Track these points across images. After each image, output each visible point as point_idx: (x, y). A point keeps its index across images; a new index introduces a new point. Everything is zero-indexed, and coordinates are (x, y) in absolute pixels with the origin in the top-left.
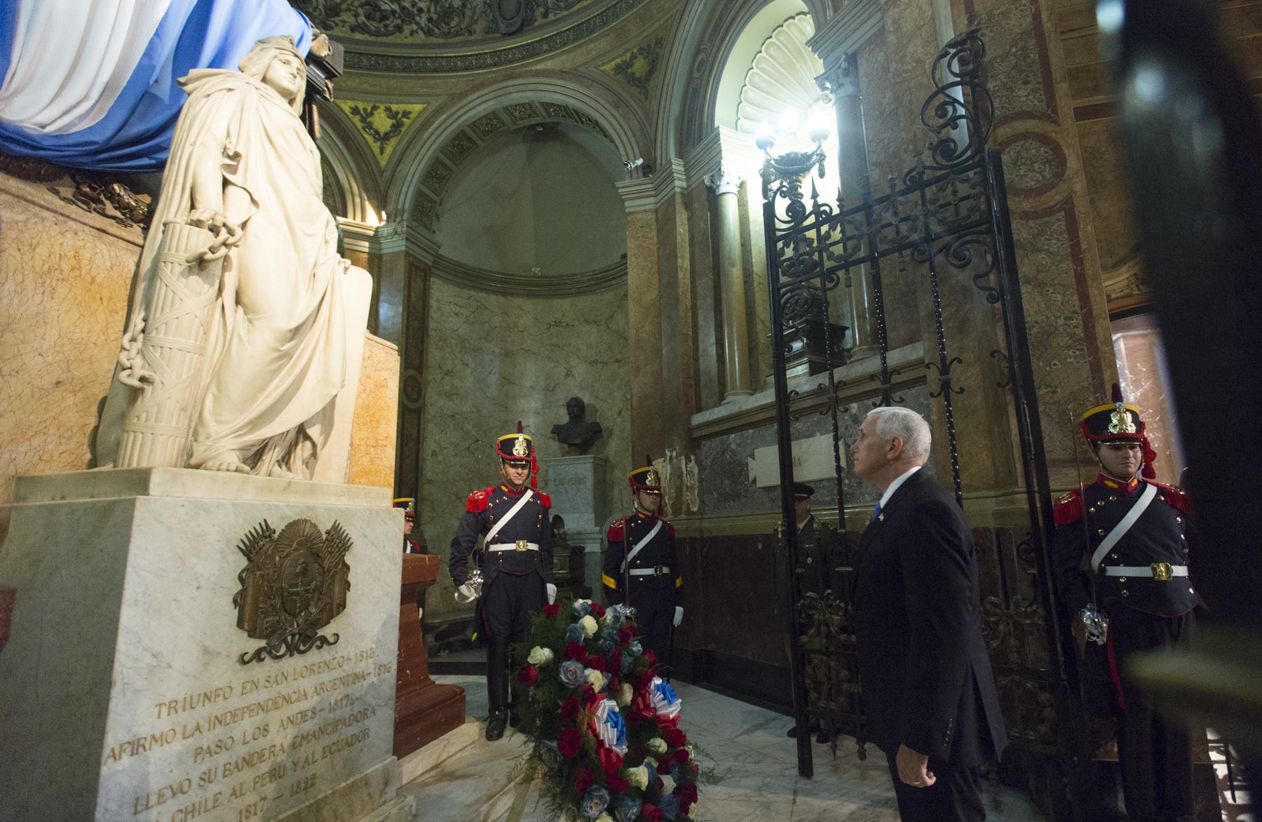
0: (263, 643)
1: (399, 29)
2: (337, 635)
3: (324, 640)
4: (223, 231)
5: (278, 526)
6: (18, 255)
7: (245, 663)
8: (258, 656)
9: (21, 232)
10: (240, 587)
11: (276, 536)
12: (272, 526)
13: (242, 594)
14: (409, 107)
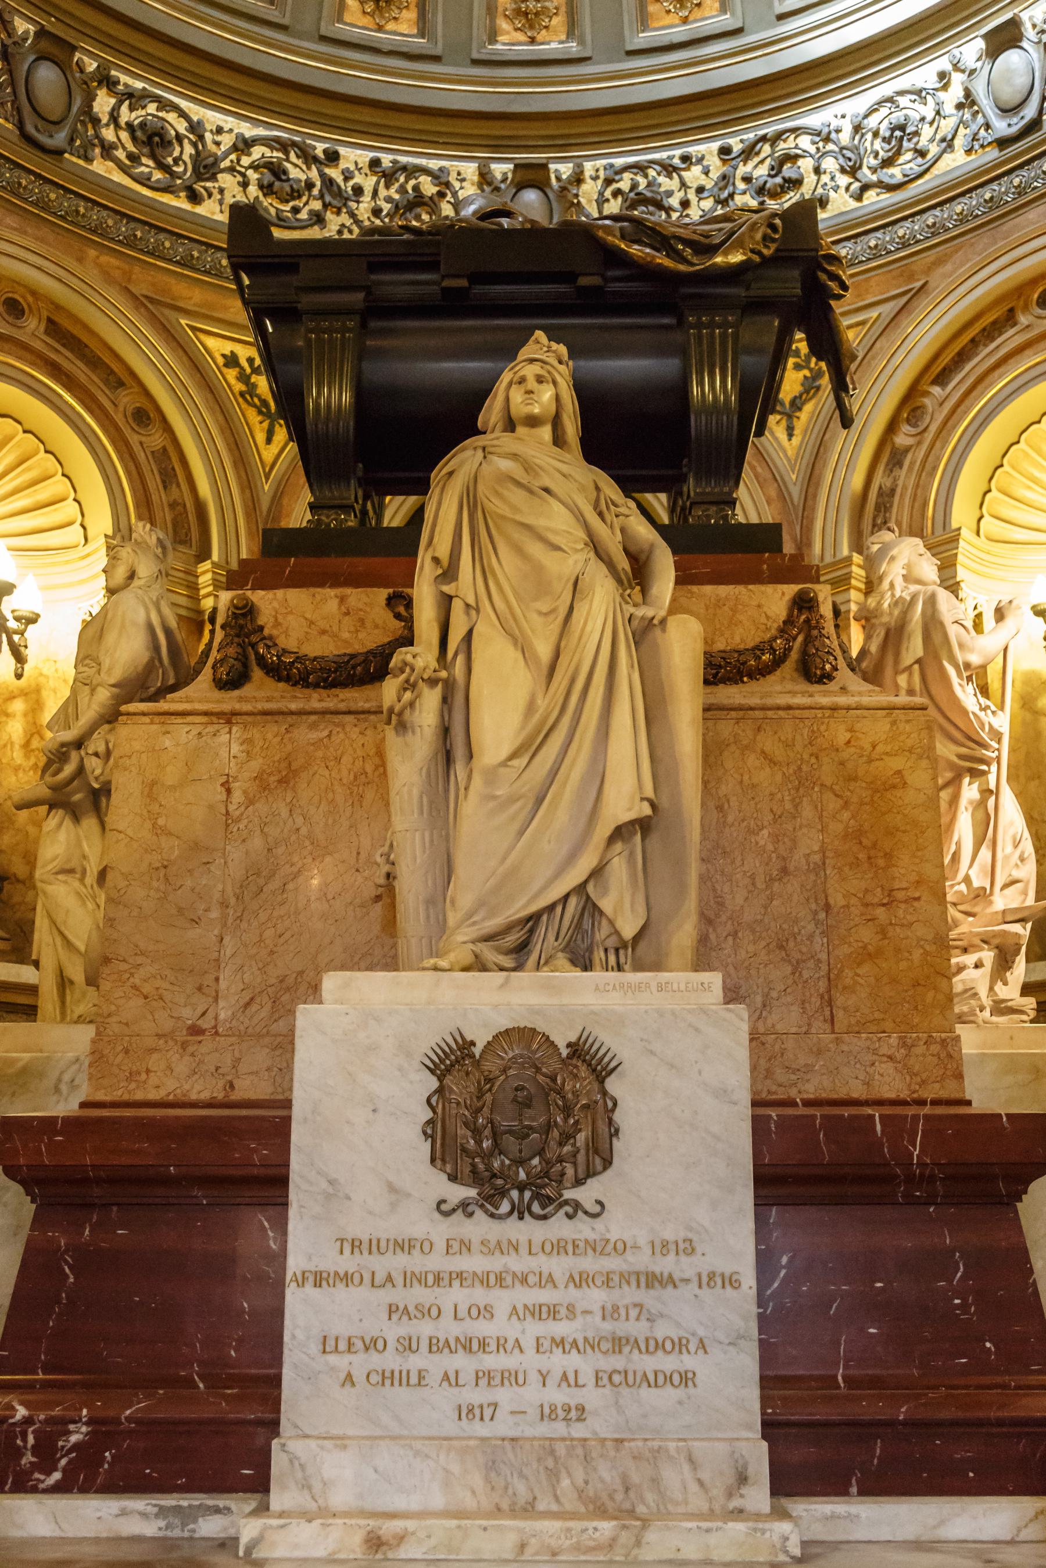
0: (472, 1193)
2: (600, 1203)
3: (577, 1206)
4: (408, 670)
5: (481, 1039)
6: (327, 773)
7: (447, 1214)
9: (327, 747)
10: (431, 1115)
11: (477, 1051)
12: (469, 1038)
13: (430, 1122)
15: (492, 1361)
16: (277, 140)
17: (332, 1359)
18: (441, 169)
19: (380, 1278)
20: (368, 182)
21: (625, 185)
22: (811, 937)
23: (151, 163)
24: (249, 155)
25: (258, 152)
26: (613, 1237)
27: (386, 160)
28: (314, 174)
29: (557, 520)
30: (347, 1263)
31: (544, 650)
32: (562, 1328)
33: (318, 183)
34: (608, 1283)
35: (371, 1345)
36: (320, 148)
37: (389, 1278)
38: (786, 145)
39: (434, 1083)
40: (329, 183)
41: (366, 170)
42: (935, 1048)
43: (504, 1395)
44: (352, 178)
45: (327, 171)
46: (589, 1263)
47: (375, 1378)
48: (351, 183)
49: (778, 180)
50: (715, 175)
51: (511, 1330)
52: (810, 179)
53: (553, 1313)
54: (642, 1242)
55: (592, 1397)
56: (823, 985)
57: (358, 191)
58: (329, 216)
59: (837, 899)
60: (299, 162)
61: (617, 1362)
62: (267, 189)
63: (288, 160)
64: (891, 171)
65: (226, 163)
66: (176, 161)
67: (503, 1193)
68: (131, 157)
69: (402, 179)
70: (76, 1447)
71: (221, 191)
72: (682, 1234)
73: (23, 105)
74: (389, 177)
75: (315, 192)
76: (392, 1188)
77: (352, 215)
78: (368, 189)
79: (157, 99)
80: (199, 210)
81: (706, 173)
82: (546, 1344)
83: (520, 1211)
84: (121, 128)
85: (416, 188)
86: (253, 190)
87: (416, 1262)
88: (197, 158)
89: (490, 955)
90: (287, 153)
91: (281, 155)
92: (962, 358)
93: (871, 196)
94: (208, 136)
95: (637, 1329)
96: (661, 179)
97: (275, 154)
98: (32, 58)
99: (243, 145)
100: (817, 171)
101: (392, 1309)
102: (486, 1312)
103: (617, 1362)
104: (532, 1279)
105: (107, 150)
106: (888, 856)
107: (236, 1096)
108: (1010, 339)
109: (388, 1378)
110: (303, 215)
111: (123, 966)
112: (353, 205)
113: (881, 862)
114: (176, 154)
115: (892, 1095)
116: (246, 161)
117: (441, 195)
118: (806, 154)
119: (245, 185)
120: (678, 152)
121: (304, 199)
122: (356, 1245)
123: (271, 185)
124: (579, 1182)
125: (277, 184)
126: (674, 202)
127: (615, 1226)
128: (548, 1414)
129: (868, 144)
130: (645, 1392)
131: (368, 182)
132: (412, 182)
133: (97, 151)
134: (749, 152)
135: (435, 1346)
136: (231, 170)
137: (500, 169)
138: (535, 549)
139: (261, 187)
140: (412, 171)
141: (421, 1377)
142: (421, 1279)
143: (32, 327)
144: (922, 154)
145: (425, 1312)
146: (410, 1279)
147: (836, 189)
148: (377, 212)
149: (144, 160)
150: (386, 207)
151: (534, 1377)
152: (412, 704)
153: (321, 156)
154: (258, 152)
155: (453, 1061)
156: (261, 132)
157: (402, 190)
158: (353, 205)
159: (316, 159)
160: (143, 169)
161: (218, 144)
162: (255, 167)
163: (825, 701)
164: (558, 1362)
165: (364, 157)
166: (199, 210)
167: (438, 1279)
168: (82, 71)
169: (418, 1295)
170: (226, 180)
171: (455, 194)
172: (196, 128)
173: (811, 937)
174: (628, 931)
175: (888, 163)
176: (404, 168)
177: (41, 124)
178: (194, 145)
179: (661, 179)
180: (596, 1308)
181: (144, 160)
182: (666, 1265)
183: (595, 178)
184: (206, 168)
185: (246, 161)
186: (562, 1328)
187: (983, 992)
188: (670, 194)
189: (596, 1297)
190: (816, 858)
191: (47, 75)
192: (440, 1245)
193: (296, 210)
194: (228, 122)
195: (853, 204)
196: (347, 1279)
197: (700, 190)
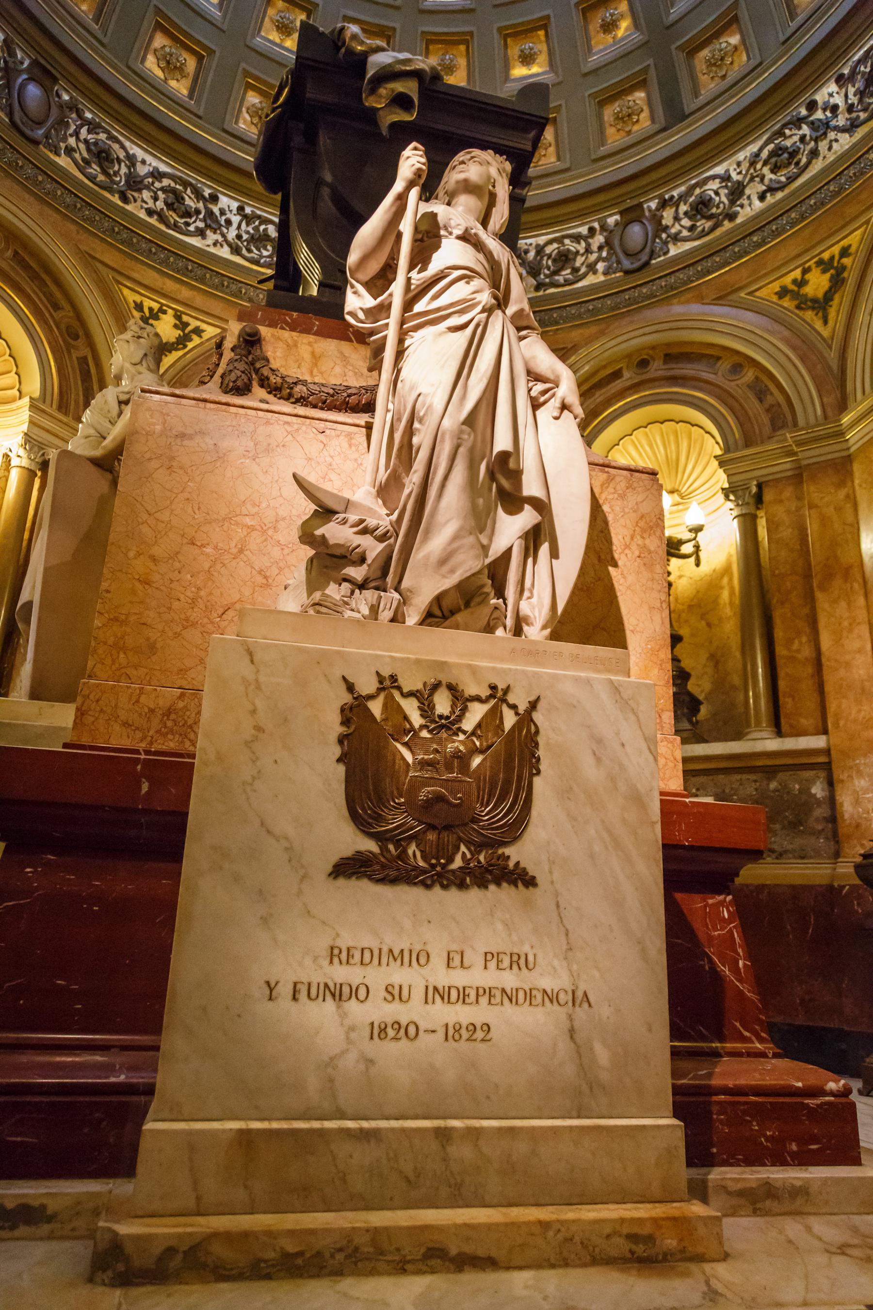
16: (180, 178)
20: (236, 219)
23: (98, 169)
24: (161, 182)
25: (166, 182)
27: (248, 210)
28: (201, 205)
33: (203, 211)
36: (207, 192)
40: (210, 214)
44: (225, 214)
45: (210, 206)
48: (224, 218)
57: (229, 222)
58: (208, 232)
60: (193, 196)
62: (169, 206)
63: (185, 193)
64: (557, 278)
68: (83, 159)
69: (257, 223)
73: (14, 104)
74: (248, 219)
75: (201, 216)
78: (235, 225)
79: (106, 131)
84: (80, 141)
85: (265, 230)
86: (160, 204)
90: (186, 190)
91: (181, 188)
97: (178, 187)
98: (25, 76)
99: (157, 175)
105: (69, 151)
110: (192, 228)
112: (225, 231)
119: (156, 199)
121: (193, 219)
123: (173, 204)
129: (544, 262)
131: (236, 219)
132: (262, 227)
139: (166, 203)
148: (239, 237)
150: (245, 237)
153: (207, 196)
154: (166, 182)
157: (256, 229)
158: (225, 231)
159: (203, 197)
160: (92, 171)
175: (556, 273)
176: (259, 217)
177: (25, 119)
185: (157, 185)
191: (33, 91)
193: (187, 224)
194: (149, 159)
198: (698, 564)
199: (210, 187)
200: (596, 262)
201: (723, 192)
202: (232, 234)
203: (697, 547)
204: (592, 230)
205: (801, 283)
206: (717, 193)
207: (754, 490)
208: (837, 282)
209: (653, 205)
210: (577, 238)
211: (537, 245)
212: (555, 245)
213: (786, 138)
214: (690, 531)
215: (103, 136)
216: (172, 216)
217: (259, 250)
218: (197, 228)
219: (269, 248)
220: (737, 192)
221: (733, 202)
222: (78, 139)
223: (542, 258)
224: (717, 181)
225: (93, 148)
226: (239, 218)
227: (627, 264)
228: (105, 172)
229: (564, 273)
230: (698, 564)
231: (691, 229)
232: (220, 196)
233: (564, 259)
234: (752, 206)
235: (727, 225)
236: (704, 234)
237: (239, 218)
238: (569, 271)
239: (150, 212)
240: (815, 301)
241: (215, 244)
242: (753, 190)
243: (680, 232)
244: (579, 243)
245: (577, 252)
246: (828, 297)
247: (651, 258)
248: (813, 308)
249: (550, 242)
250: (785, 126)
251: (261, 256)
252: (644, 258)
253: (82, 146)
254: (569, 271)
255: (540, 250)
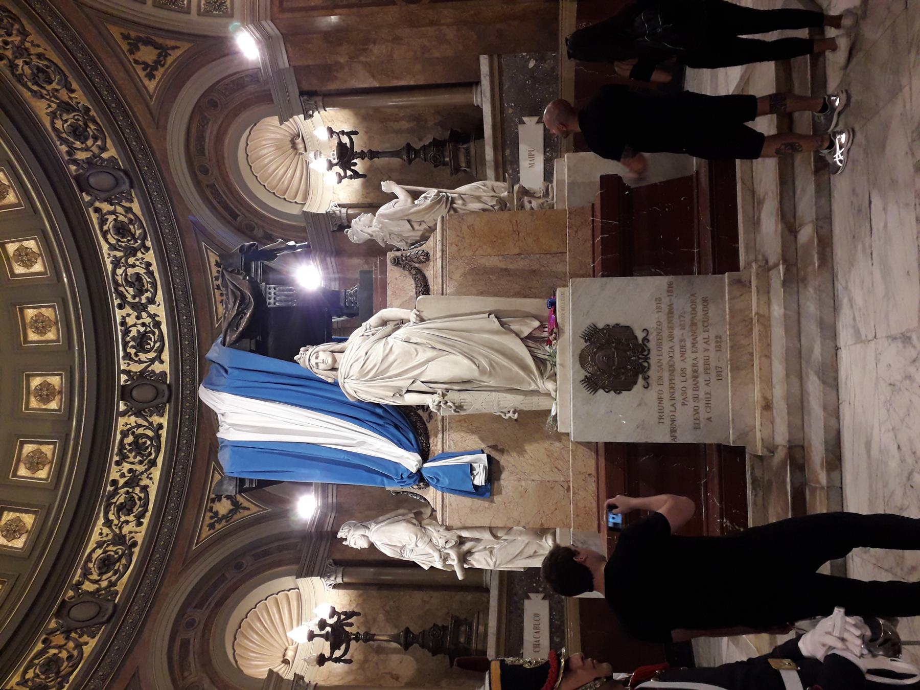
0: (640, 376)
1: (40, 56)
3: (646, 339)
8: (646, 379)
12: (583, 378)
14: (118, 38)
15: (701, 369)
17: (702, 425)
18: (122, 432)
19: (673, 409)
21: (133, 351)
22: (531, 260)
23: (118, 564)
26: (655, 326)
27: (116, 458)
29: (378, 351)
30: (667, 421)
31: (430, 353)
32: (688, 345)
34: (672, 328)
35: (696, 411)
36: (109, 488)
37: (673, 405)
38: (119, 279)
39: (601, 391)
40: (126, 484)
41: (120, 467)
42: (573, 216)
43: (713, 364)
45: (120, 485)
46: (665, 334)
47: (708, 410)
48: (127, 474)
49: (136, 283)
50: (131, 311)
51: (689, 361)
52: (137, 270)
53: (683, 347)
54: (657, 316)
55: (712, 333)
56: (548, 256)
57: (130, 471)
59: (517, 251)
61: (700, 325)
64: (137, 235)
65: (117, 531)
66: (116, 553)
67: (642, 365)
68: (115, 574)
70: (731, 523)
71: (131, 532)
72: (654, 302)
74: (124, 457)
75: (131, 490)
76: (639, 405)
77: (142, 473)
78: (130, 466)
80: (140, 542)
81: (129, 315)
82: (694, 349)
83: (647, 358)
86: (131, 518)
87: (666, 396)
88: (114, 544)
89: (547, 374)
92: (226, 207)
93: (148, 243)
94: (105, 539)
95: (688, 318)
96: (131, 335)
99: (108, 523)
100: (134, 266)
101: (683, 404)
102: (683, 370)
103: (700, 325)
104: (671, 354)
105: (112, 584)
106: (500, 232)
107: (594, 472)
108: (221, 187)
109: (708, 404)
110: (142, 495)
111: (544, 518)
113: (503, 235)
114: (113, 553)
115: (590, 232)
116: (116, 522)
117: (133, 433)
118: (125, 271)
119: (127, 522)
120: (119, 327)
122: (661, 418)
123: (128, 510)
124: (636, 338)
125: (128, 507)
126: (142, 329)
127: (651, 325)
128: (719, 349)
130: (710, 315)
131: (126, 467)
133: (112, 589)
134: (122, 296)
135: (696, 388)
136: (121, 528)
137: (122, 407)
138: (391, 358)
139: (129, 515)
140: (122, 445)
141: (707, 394)
142: (673, 394)
143: (200, 616)
144: (131, 221)
145: (684, 392)
146: (672, 398)
147: (143, 259)
148: (141, 462)
149: (116, 568)
150: (139, 458)
151: (706, 354)
152: (454, 403)
154: (111, 517)
155: (592, 383)
156: (102, 515)
157: (130, 451)
160: (121, 568)
161: (107, 535)
162: (119, 518)
163: (439, 254)
164: (701, 345)
165: (114, 468)
166: (140, 542)
167: (672, 388)
168: (74, 597)
169: (678, 395)
170: (126, 530)
171: (133, 427)
172: (99, 545)
173: (531, 260)
174: (536, 324)
175: (133, 236)
178: (108, 545)
179: (131, 335)
180: (681, 332)
181: (116, 568)
182: (665, 307)
183: (129, 365)
184: (119, 539)
185: (116, 522)
186: (688, 345)
187: (541, 201)
188: (138, 331)
189: (677, 332)
190: (501, 258)
192: (660, 387)
193: (140, 499)
194: (97, 530)
195: (151, 252)
196: (673, 421)
197: (138, 318)
198: (356, 133)
199: (106, 487)
200: (123, 206)
201: (65, 117)
202: (140, 468)
203: (343, 133)
204: (97, 210)
205: (146, 65)
206: (66, 121)
207: (305, 97)
208: (148, 42)
209: (73, 168)
210: (103, 221)
211: (109, 249)
212: (109, 236)
213: (23, 74)
214: (332, 137)
215: (91, 565)
216: (137, 509)
217: (147, 448)
218: (141, 492)
219: (144, 440)
220: (66, 107)
221: (74, 110)
222: (100, 580)
223: (120, 246)
224: (55, 121)
225: (104, 570)
226: (125, 464)
227: (126, 187)
228: (119, 559)
229: (133, 230)
230: (356, 133)
231: (95, 138)
232: (111, 479)
233: (121, 230)
234: (80, 97)
235: (92, 113)
236: (100, 129)
237: (125, 464)
238: (131, 227)
239: (140, 524)
240: (160, 55)
241: (151, 479)
242: (64, 95)
243: (99, 146)
244: (107, 219)
245: (115, 220)
246: (157, 46)
247: (120, 169)
248: (166, 56)
249: (107, 241)
250: (13, 74)
251: (152, 445)
252: (122, 174)
253: (104, 577)
254: (131, 227)
255: (113, 247)
